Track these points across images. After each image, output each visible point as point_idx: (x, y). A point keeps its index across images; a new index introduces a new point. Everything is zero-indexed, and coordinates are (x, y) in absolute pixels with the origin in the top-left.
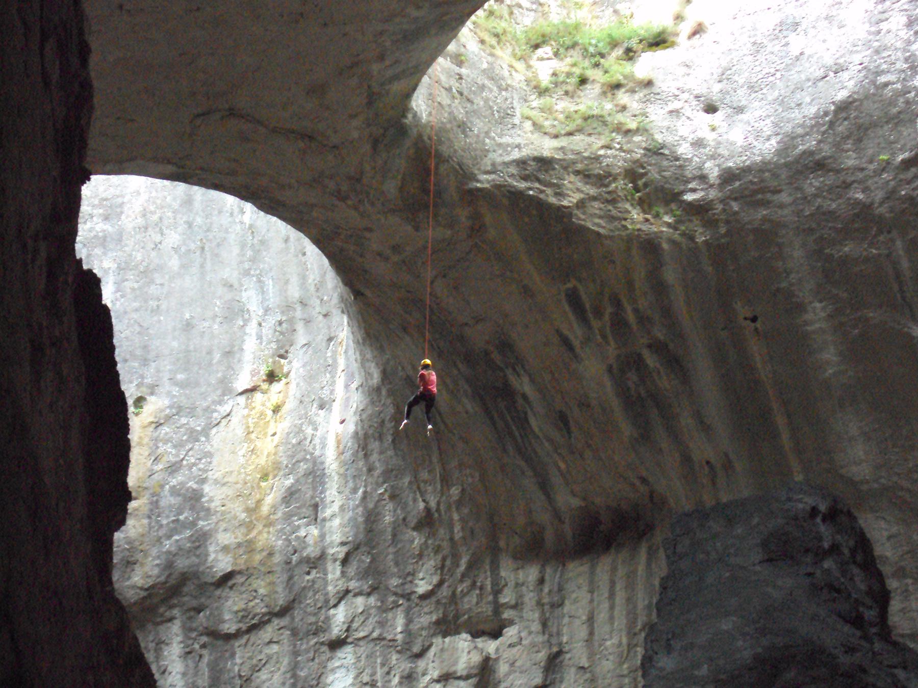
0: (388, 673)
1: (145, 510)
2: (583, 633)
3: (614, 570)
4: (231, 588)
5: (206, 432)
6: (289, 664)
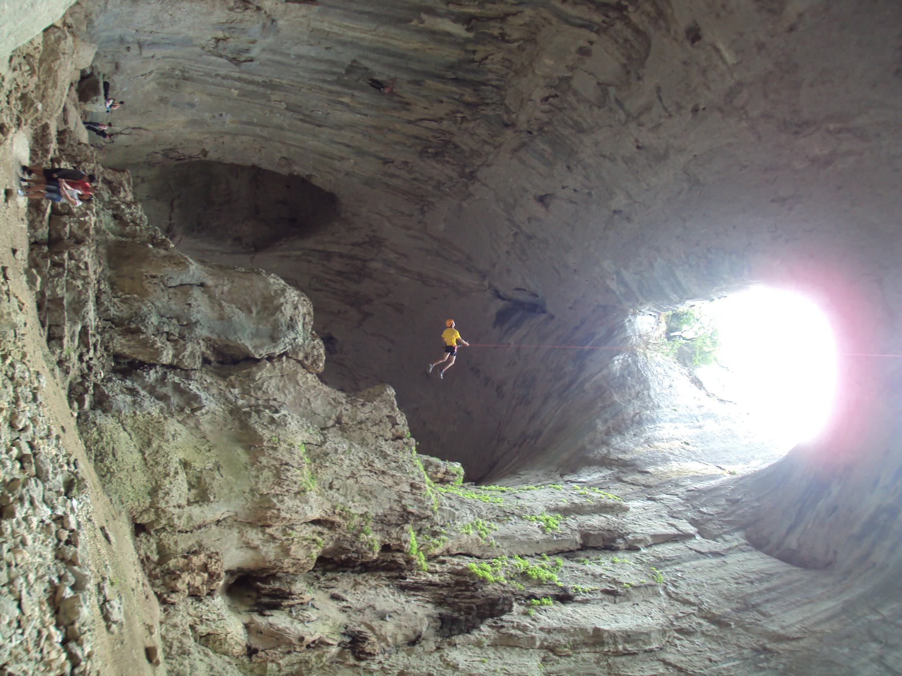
5: (693, 460)
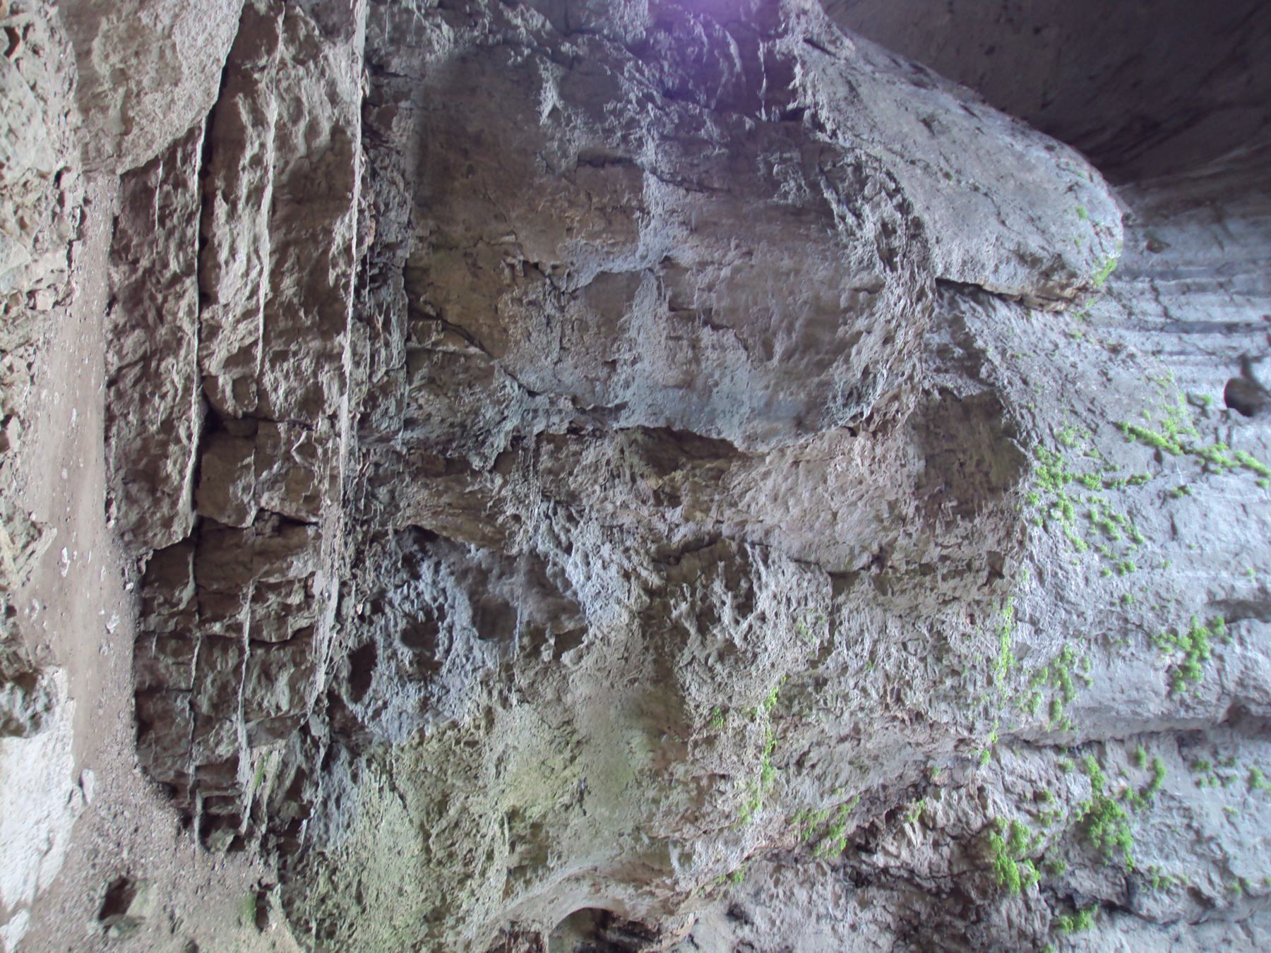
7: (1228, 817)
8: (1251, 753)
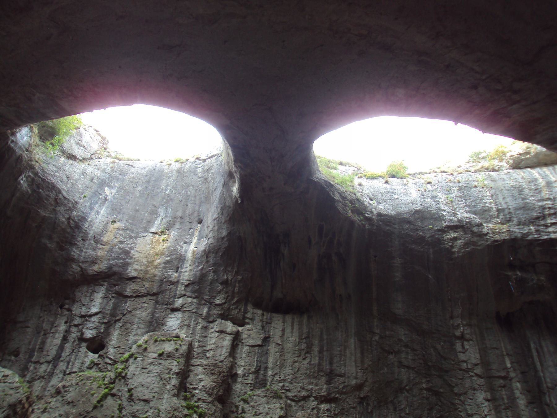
0: (196, 324)
1: (107, 250)
2: (280, 334)
3: (293, 319)
4: (133, 282)
5: (136, 238)
6: (151, 311)
7: (257, 415)
8: (235, 398)
